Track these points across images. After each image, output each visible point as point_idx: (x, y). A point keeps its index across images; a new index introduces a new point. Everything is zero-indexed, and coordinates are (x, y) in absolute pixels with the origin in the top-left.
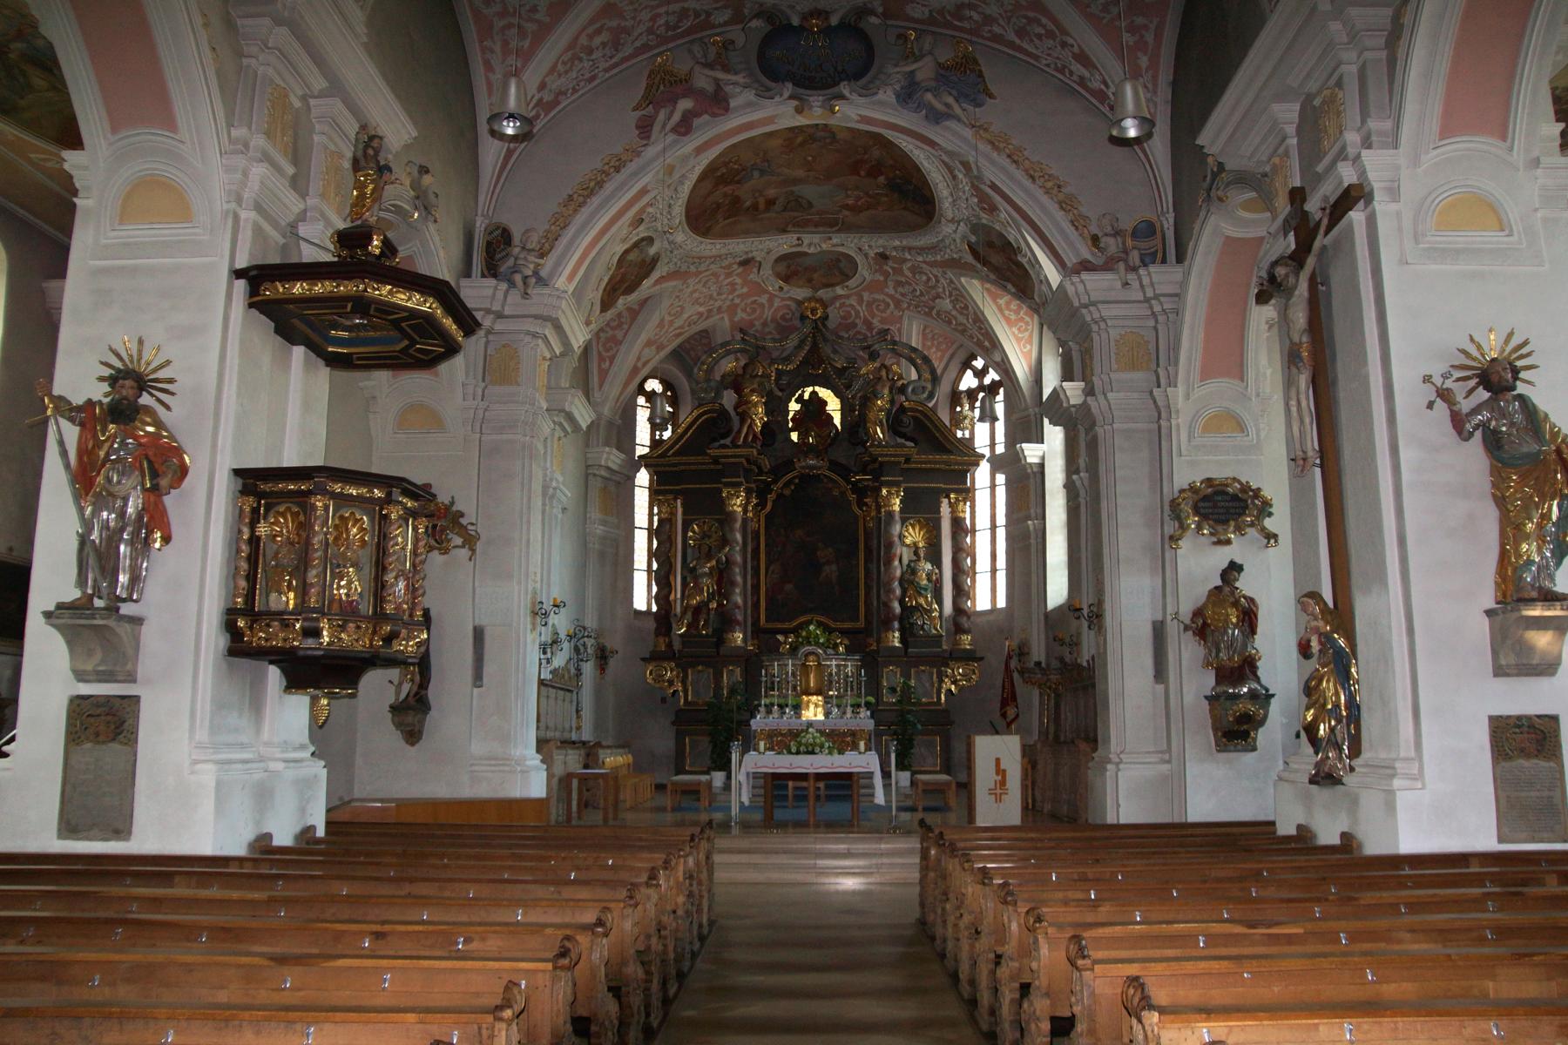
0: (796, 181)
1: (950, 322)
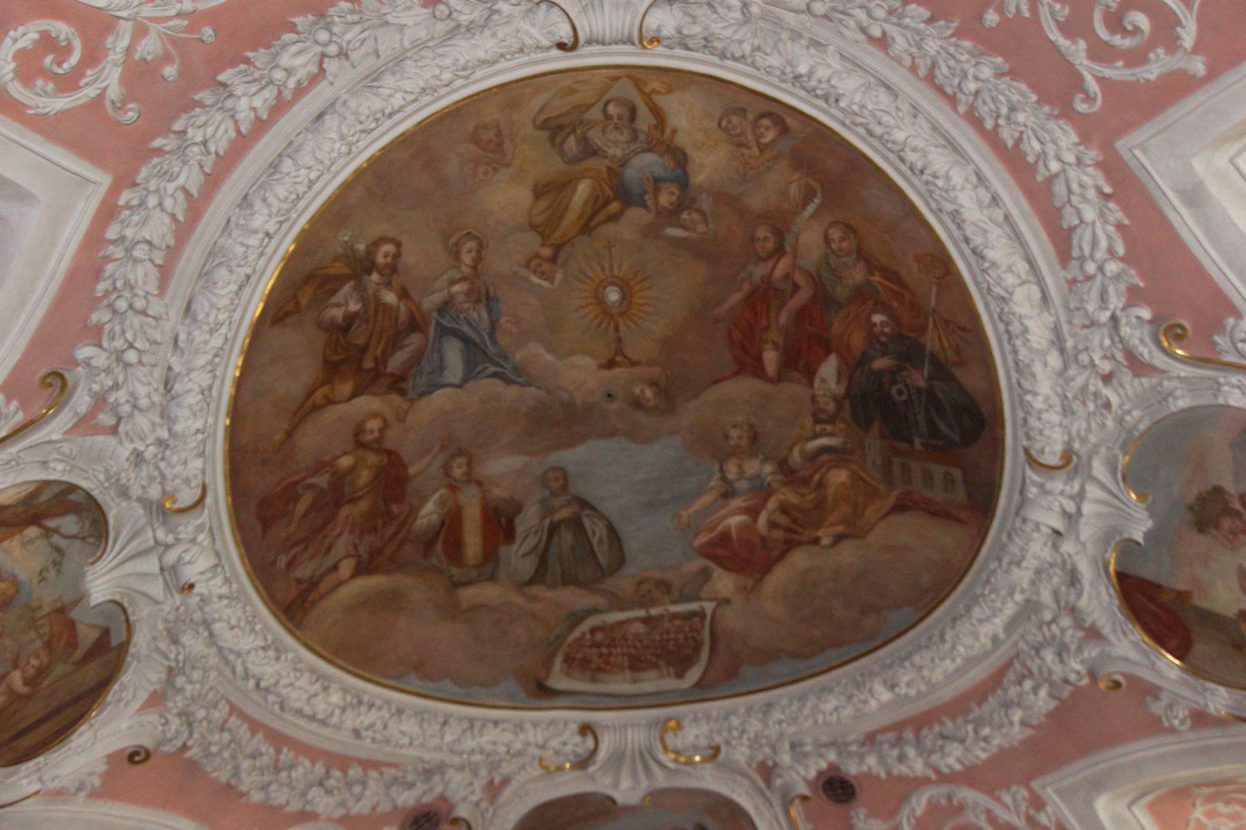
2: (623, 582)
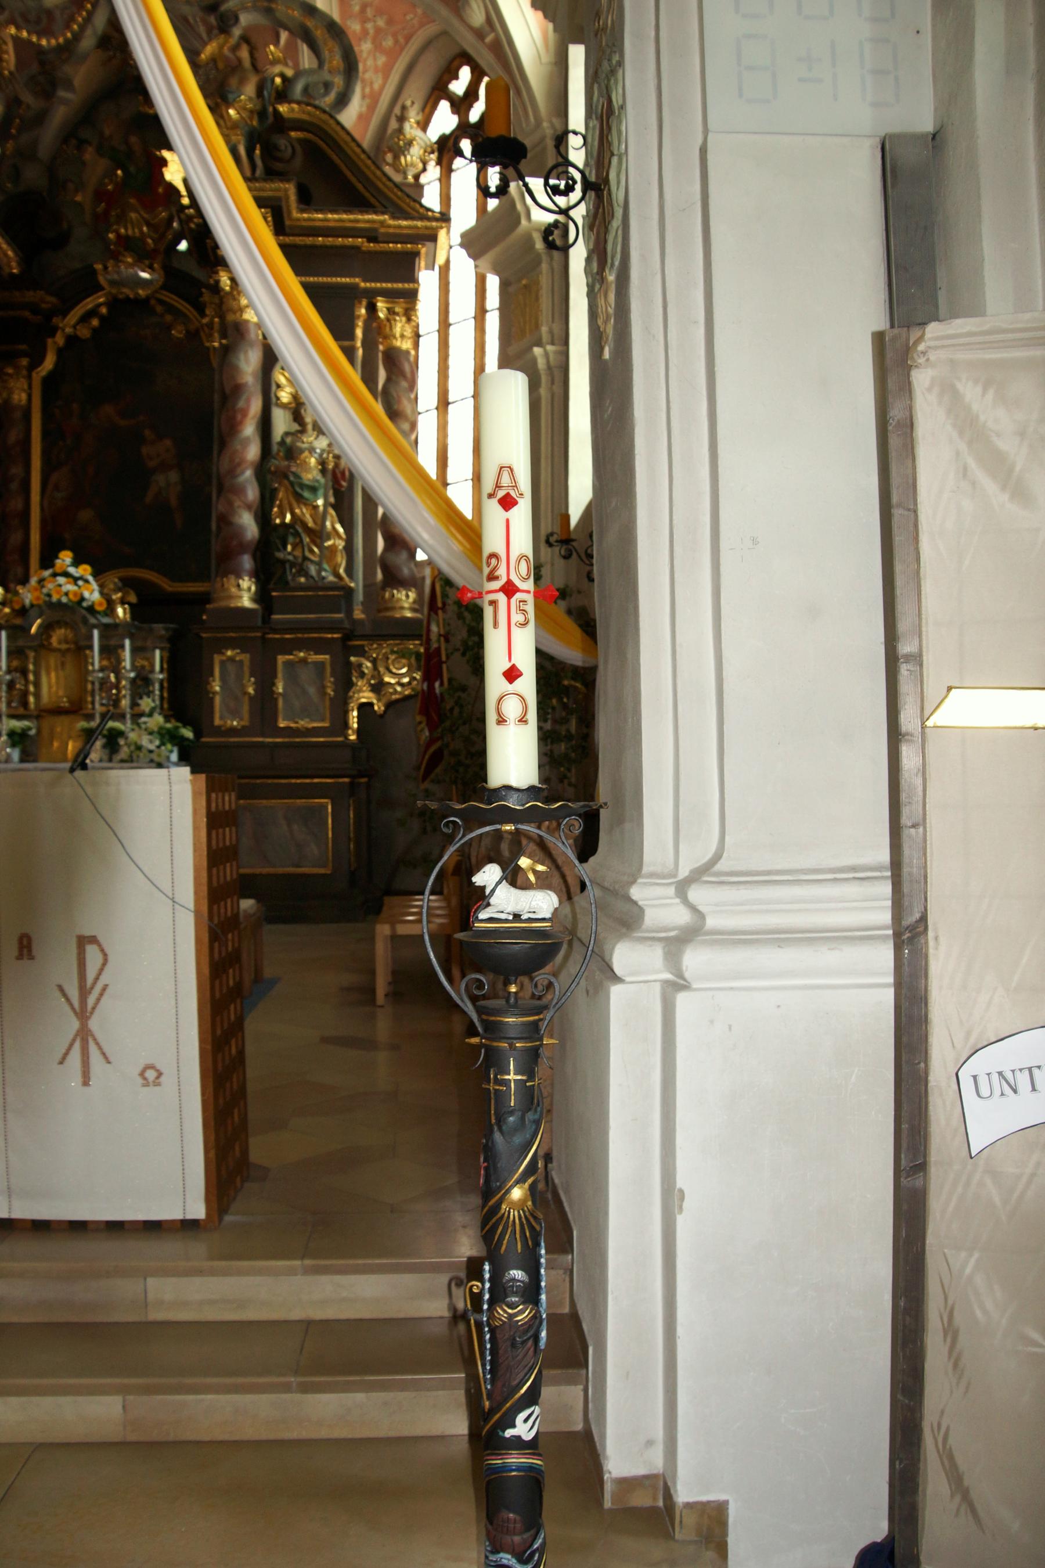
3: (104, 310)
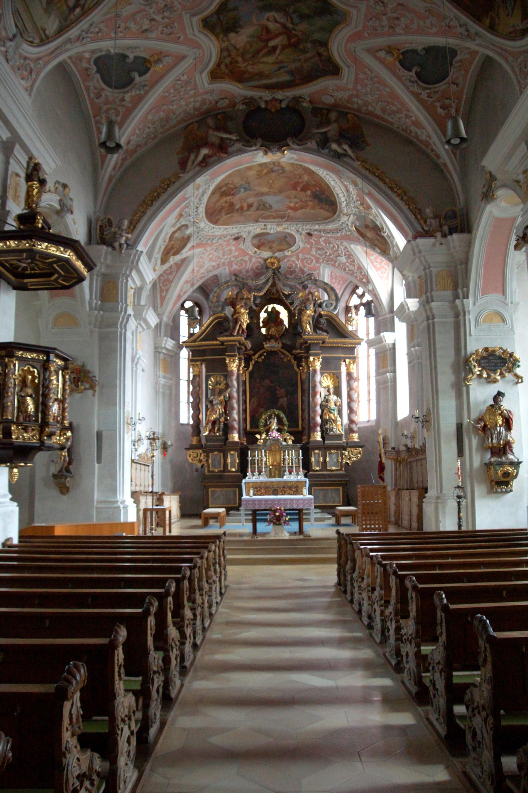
0: (263, 194)
1: (345, 270)
2: (273, 210)
3: (265, 354)
